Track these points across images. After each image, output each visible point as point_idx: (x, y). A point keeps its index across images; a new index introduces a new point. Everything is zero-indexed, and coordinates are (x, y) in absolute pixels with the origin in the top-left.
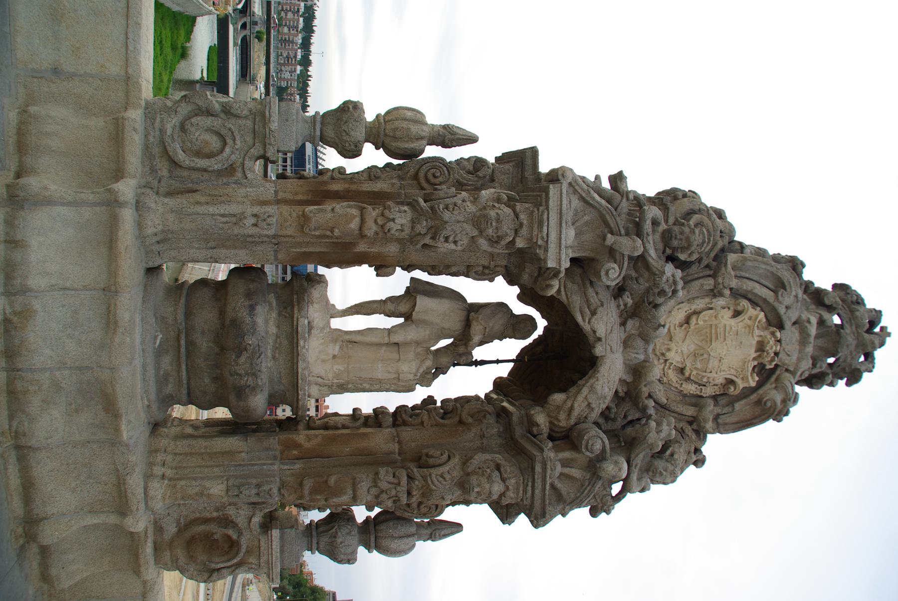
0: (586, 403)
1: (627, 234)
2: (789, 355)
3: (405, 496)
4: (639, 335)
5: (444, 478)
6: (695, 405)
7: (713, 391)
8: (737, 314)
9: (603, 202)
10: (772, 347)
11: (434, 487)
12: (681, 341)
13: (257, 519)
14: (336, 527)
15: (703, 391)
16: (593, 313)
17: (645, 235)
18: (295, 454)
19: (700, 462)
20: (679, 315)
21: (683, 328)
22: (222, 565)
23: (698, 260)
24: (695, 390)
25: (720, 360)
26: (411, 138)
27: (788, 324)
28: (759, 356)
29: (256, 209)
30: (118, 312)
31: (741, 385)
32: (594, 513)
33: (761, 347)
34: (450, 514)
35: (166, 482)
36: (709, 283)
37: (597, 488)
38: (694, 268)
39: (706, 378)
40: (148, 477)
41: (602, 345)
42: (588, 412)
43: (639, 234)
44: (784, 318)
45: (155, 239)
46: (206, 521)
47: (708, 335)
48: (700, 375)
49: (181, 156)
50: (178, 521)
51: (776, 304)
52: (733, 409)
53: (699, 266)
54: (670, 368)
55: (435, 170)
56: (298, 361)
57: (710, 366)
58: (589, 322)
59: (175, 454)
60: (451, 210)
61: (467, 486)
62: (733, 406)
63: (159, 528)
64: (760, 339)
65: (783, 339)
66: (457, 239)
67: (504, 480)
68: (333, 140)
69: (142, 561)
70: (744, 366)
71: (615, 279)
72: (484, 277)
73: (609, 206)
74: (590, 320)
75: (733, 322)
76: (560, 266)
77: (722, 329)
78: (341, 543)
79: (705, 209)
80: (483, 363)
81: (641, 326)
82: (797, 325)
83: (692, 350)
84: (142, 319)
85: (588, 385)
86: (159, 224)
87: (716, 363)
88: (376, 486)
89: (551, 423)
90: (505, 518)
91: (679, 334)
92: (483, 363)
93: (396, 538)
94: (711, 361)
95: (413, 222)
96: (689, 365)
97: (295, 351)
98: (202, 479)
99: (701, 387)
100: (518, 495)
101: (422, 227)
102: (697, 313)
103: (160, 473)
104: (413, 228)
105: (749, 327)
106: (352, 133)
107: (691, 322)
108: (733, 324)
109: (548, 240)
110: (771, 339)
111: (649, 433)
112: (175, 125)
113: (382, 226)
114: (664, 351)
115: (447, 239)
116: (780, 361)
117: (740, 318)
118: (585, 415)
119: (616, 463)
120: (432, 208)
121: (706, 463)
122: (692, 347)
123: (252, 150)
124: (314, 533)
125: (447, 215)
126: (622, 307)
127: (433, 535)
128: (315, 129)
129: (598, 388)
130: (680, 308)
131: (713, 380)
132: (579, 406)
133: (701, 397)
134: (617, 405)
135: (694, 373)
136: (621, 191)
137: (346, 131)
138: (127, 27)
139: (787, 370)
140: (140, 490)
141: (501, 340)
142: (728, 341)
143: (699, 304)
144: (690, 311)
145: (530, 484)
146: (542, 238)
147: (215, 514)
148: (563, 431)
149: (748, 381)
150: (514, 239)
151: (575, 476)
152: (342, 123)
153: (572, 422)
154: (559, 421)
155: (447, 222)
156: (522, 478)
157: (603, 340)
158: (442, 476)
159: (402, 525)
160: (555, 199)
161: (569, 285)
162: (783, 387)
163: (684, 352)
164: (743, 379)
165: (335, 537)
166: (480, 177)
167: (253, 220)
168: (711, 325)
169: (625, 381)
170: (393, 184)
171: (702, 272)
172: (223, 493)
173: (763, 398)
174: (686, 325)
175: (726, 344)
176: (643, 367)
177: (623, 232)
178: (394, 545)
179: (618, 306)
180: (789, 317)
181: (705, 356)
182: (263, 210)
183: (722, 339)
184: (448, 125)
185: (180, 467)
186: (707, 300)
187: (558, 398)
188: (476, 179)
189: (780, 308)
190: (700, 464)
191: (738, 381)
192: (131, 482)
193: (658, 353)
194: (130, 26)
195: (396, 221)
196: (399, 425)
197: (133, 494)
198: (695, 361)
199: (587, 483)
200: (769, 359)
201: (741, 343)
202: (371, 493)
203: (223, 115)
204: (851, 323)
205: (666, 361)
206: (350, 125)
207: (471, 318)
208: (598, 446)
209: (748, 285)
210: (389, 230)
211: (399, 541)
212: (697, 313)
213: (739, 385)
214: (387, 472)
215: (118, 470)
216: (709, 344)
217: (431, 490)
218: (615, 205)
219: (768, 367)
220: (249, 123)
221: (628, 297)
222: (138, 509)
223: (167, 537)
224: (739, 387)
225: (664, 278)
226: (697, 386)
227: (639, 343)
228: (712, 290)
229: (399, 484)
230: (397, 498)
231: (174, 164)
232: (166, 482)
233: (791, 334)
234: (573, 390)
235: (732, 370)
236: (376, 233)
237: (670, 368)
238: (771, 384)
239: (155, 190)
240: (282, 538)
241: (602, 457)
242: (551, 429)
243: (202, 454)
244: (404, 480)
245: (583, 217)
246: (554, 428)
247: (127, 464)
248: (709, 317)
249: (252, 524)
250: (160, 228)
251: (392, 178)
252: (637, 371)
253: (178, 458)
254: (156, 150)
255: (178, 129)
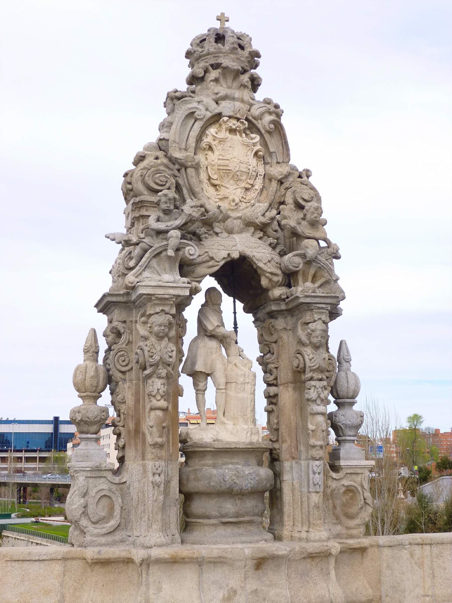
0: (268, 263)
1: (167, 239)
2: (239, 110)
3: (322, 382)
4: (224, 222)
5: (312, 358)
6: (270, 180)
7: (261, 166)
8: (210, 148)
9: (147, 255)
10: (233, 123)
11: (317, 366)
12: (228, 190)
13: (334, 475)
14: (340, 424)
15: (261, 174)
16: (212, 258)
17: (167, 228)
18: (295, 450)
19: (308, 173)
20: (211, 190)
21: (219, 189)
22: (362, 497)
23: (175, 178)
24: (260, 179)
25: (242, 163)
26: (97, 375)
27: (217, 110)
28: (239, 131)
29: (150, 475)
30: (214, 556)
31: (258, 147)
33: (232, 131)
34: (334, 351)
35: (311, 530)
36: (191, 171)
37: (322, 259)
38: (181, 182)
39: (253, 173)
40: (308, 540)
41: (233, 253)
42: (273, 262)
43: (167, 232)
44: (213, 113)
45: (166, 537)
46: (335, 507)
47: (224, 171)
48: (250, 177)
49: (113, 523)
50: (334, 524)
51: (205, 120)
52: (274, 152)
53: (179, 177)
54: (245, 198)
55: (120, 361)
56: (239, 448)
57: (245, 170)
58: (218, 262)
59: (294, 525)
60: (153, 354)
61: (317, 345)
62: (272, 152)
63: (338, 536)
64: (228, 132)
65: (228, 114)
66: (170, 350)
67: (315, 321)
68: (99, 427)
69: (358, 546)
70: (246, 145)
71: (195, 249)
72: (184, 325)
73: (149, 251)
74: (216, 261)
75: (217, 153)
76: (189, 287)
77: (221, 161)
78: (350, 421)
79: (141, 171)
81: (219, 222)
82: (219, 102)
83: (234, 182)
84: (214, 544)
85: (257, 262)
86: (159, 534)
87: (244, 165)
88: (315, 401)
89: (279, 286)
90: (338, 315)
91: (223, 192)
93: (348, 386)
94: (242, 169)
95: (159, 378)
96: (243, 185)
97: (234, 450)
98: (309, 507)
99: (258, 175)
100: (324, 313)
101: (163, 372)
102: (209, 179)
103: (306, 533)
104: (163, 378)
105: (220, 141)
106: (96, 413)
107: (216, 184)
108: (218, 153)
109: (173, 295)
110: (228, 125)
111: (289, 225)
112: (94, 528)
113: (162, 397)
114: (234, 204)
115: (171, 357)
116: (243, 116)
117: (214, 147)
118: (275, 264)
120: (151, 366)
121: (308, 168)
122: (232, 182)
123: (109, 478)
124: (344, 438)
125: (157, 358)
126: (206, 235)
127: (347, 360)
128: (92, 438)
129: (259, 255)
130: (206, 191)
131: (254, 168)
132: (270, 268)
133: (264, 174)
134: (269, 237)
135: (249, 181)
136: (138, 242)
137: (94, 418)
138: (31, 560)
139: (249, 111)
140: (316, 544)
141: (222, 312)
142: (228, 157)
144: (208, 184)
145: (318, 305)
146: (172, 298)
147: (330, 501)
148: (285, 278)
149: (256, 143)
150: (170, 315)
151: (313, 273)
152: (89, 420)
153: (279, 272)
154: (278, 281)
155: (161, 357)
156: (314, 310)
157: (229, 252)
158: (311, 360)
159: (340, 381)
160: (148, 290)
161: (195, 275)
162: (261, 115)
163: (235, 188)
164: (254, 146)
165: (346, 425)
166: (124, 331)
167: (157, 477)
168: (218, 169)
169: (253, 233)
170: (129, 387)
171: (183, 175)
172: (318, 495)
173: (268, 130)
174: (217, 187)
175: (231, 159)
176: (245, 220)
177: (165, 243)
179: (206, 238)
181: (238, 173)
182: (150, 470)
183: (228, 162)
184: (84, 349)
185: (302, 522)
186: (201, 171)
187: (264, 282)
188: (125, 333)
189: (208, 116)
190: (309, 173)
191: (256, 149)
192: (311, 550)
193: (236, 207)
194: (31, 559)
195: (159, 388)
196: (277, 383)
197: (318, 548)
198: (241, 180)
199: (319, 265)
200: (241, 125)
201: (230, 147)
202: (319, 403)
203: (86, 498)
204: (217, 57)
205: (240, 201)
206: (90, 415)
207: (209, 335)
209: (192, 142)
210: (164, 392)
211: (350, 383)
212: (209, 179)
213: (259, 149)
214: (307, 393)
215: (304, 558)
216: (231, 171)
217: (319, 366)
218: (147, 247)
219: (247, 126)
220: (91, 480)
221: (200, 231)
222: (327, 546)
223: (344, 531)
224: (261, 149)
225: (194, 214)
226: (257, 178)
227: (229, 222)
228: (195, 168)
229: (315, 386)
230: (323, 388)
231: (118, 528)
232: (311, 530)
233: (226, 108)
234: (259, 272)
235: (248, 154)
236: (165, 400)
237: (245, 198)
238: (258, 123)
239: (137, 538)
240: (346, 459)
242: (283, 286)
243: (293, 508)
244: (313, 383)
245: (155, 268)
246: (283, 284)
247: (300, 552)
248: (213, 171)
249: (337, 478)
250: (161, 533)
251: (124, 388)
252: (249, 224)
253: (296, 523)
254: (110, 538)
255: (96, 526)
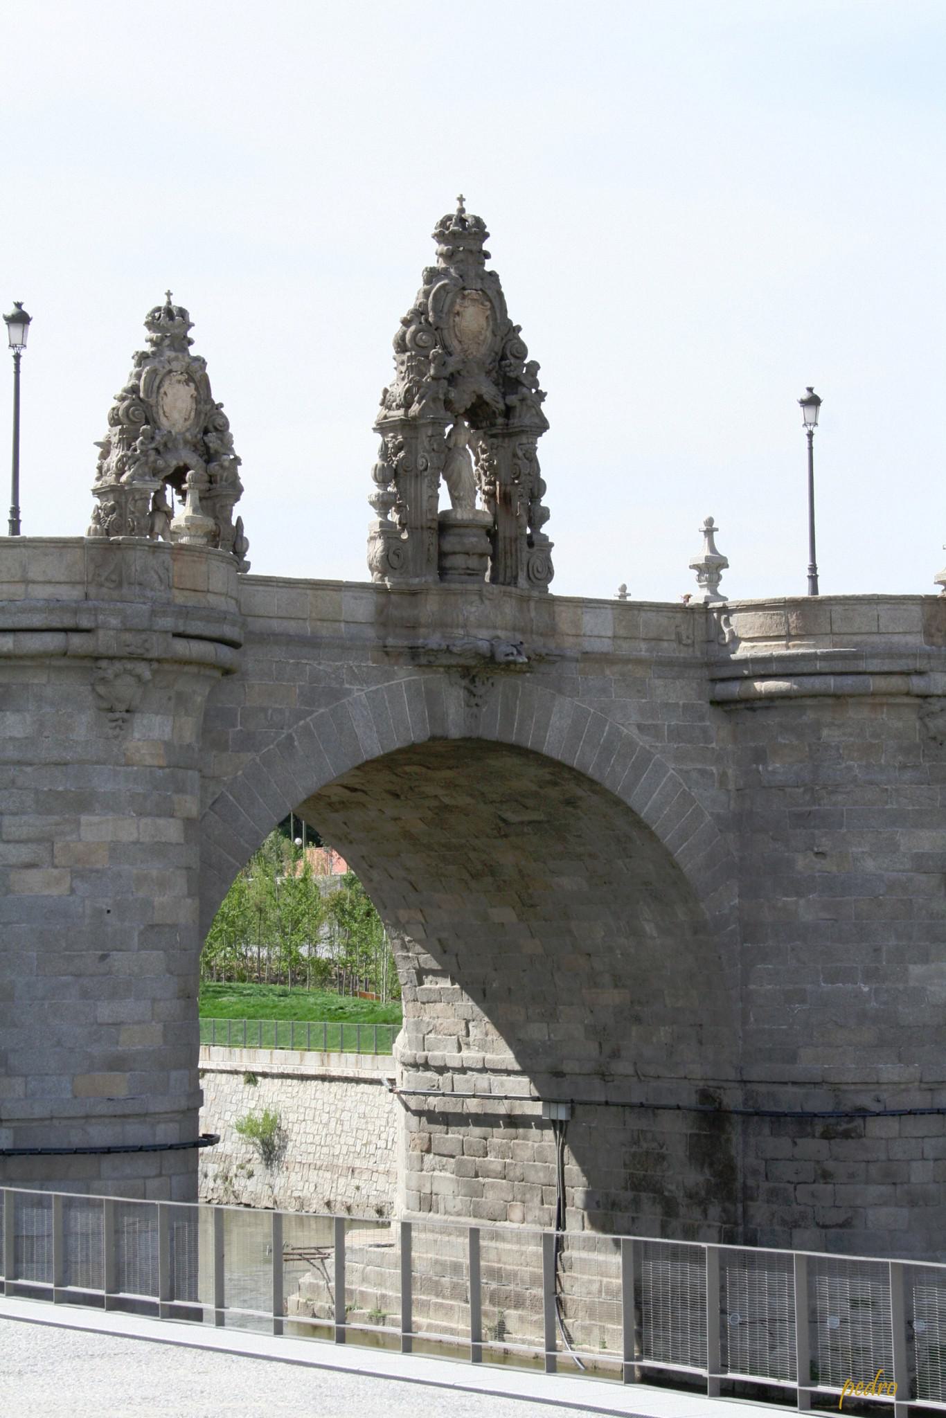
8: (165, 393)
32: (240, 464)
33: (179, 382)
34: (234, 523)
80: (173, 503)
92: (173, 503)
102: (164, 413)
119: (224, 460)
143: (161, 412)
178: (245, 546)
180: (168, 368)
208: (217, 468)
209: (155, 388)
212: (164, 413)
241: (222, 466)
